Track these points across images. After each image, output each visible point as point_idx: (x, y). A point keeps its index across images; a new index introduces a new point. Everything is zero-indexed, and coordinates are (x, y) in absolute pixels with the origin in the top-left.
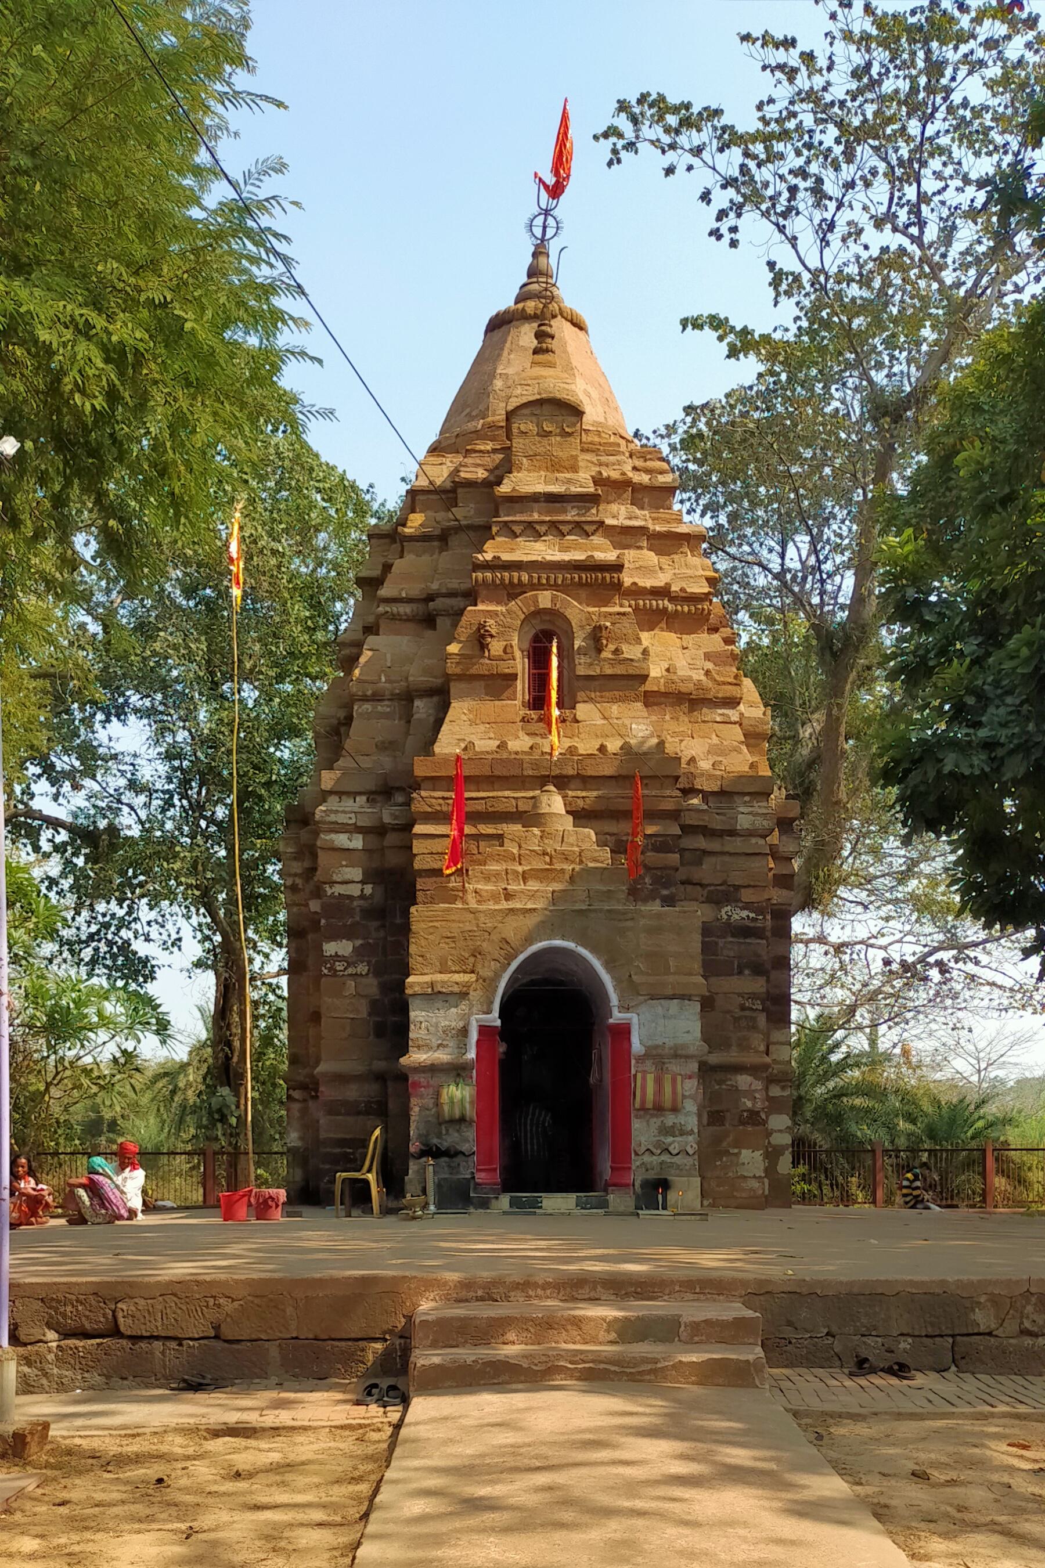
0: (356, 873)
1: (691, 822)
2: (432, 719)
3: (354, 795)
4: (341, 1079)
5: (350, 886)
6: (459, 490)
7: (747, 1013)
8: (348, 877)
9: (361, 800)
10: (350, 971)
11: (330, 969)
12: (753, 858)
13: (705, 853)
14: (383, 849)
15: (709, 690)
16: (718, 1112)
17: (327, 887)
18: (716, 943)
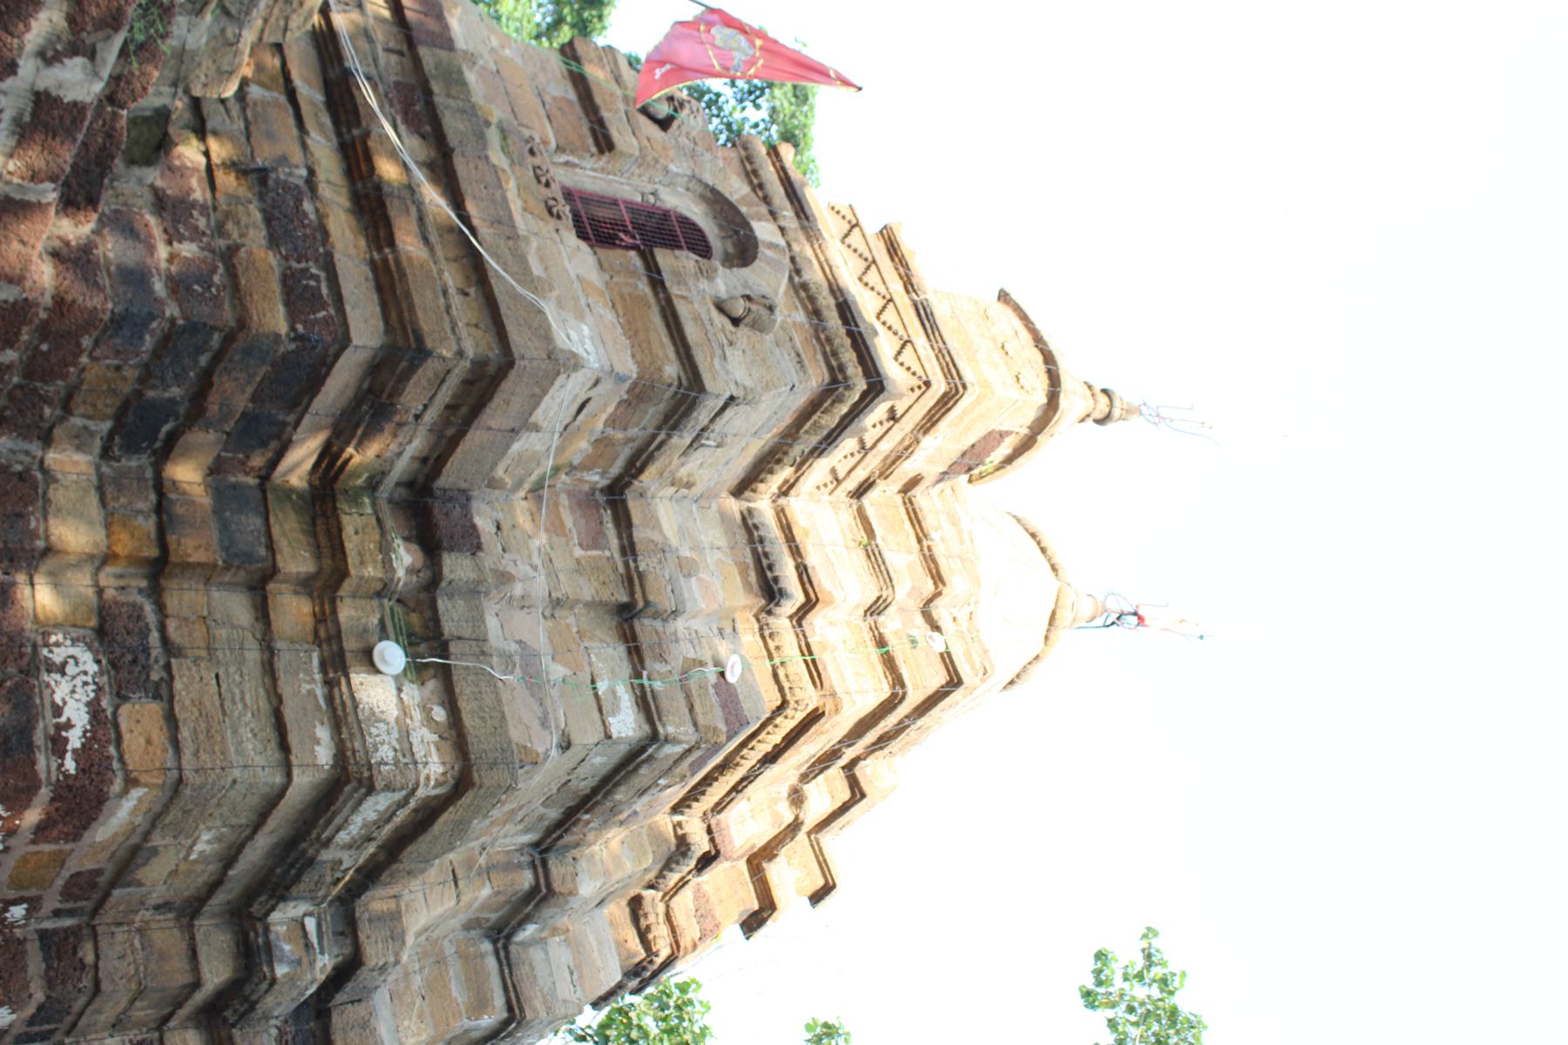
12: (270, 733)
13: (259, 588)
15: (661, 658)
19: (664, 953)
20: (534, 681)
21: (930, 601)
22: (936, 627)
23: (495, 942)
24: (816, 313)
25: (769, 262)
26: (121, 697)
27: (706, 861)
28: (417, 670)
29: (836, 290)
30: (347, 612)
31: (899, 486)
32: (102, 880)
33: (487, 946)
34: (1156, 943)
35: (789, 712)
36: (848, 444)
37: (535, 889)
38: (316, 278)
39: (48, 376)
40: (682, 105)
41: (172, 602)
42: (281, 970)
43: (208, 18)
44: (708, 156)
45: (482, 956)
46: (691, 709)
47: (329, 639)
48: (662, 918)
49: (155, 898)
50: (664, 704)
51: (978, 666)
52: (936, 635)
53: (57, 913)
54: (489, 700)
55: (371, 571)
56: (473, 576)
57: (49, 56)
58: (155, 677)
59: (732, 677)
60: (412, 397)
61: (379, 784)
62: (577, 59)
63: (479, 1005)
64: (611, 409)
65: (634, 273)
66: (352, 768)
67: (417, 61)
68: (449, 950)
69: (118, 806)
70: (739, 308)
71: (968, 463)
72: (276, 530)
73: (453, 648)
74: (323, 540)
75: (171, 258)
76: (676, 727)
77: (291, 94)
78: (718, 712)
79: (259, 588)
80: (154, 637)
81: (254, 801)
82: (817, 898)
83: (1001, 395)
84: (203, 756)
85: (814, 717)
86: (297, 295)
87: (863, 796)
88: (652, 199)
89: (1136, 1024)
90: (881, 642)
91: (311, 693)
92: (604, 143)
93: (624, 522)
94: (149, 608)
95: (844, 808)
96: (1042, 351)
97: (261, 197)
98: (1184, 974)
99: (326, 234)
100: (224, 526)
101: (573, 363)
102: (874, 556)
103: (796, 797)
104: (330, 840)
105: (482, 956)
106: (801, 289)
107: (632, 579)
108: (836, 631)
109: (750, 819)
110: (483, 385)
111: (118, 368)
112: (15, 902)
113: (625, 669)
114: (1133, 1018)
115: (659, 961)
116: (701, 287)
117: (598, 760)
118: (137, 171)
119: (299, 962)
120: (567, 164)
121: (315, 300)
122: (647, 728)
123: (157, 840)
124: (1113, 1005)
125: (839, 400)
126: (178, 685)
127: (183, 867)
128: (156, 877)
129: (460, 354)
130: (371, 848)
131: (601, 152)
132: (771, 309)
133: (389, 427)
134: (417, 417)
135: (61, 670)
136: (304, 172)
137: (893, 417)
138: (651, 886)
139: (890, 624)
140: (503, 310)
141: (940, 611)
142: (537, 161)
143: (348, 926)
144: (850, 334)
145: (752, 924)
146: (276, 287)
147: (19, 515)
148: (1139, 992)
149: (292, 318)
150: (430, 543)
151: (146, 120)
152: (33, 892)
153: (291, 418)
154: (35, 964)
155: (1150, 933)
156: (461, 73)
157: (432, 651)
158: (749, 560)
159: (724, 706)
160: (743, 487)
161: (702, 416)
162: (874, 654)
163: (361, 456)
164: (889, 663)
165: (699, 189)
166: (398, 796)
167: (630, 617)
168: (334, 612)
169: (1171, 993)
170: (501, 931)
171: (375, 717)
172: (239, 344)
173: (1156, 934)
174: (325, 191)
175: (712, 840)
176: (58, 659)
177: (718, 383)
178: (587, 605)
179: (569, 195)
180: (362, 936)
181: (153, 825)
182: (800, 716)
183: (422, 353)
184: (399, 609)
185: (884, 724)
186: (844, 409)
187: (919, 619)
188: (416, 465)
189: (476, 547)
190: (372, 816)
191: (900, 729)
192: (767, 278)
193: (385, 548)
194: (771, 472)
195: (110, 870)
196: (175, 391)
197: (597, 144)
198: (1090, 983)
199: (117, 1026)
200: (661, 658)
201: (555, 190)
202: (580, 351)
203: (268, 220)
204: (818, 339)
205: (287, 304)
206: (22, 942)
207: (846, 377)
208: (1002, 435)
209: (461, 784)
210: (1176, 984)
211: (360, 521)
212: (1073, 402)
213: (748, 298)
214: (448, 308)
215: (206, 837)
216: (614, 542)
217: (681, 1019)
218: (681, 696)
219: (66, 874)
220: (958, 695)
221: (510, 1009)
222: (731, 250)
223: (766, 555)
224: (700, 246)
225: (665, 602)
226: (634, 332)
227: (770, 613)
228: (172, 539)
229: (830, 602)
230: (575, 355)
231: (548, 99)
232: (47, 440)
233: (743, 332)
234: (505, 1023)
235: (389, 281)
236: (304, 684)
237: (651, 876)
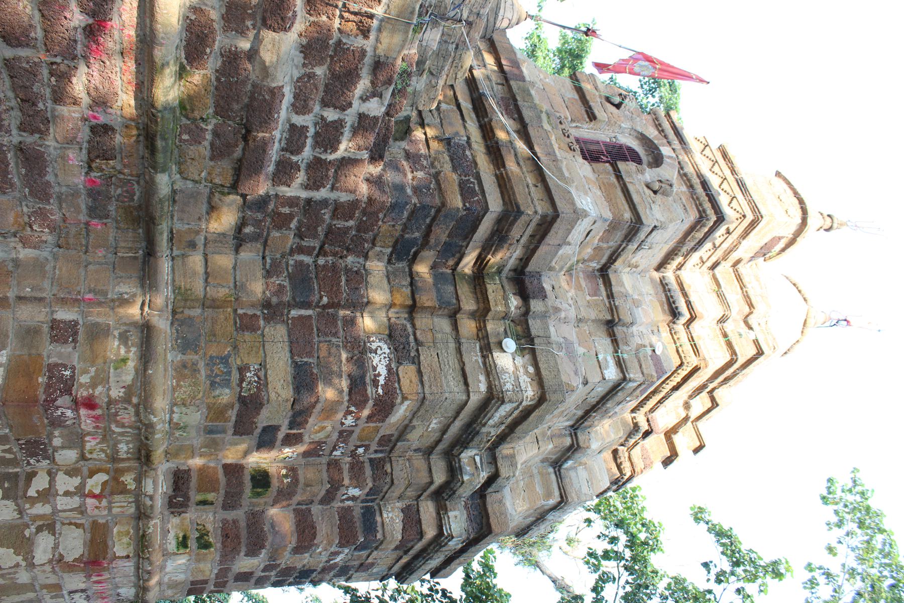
1: (490, 291)
7: (235, 376)
12: (460, 378)
13: (453, 316)
15: (627, 344)
16: (76, 333)
18: (335, 335)
19: (628, 474)
20: (571, 355)
21: (748, 316)
22: (751, 328)
23: (554, 468)
24: (691, 186)
25: (669, 164)
26: (399, 363)
27: (647, 434)
28: (521, 350)
29: (700, 176)
30: (490, 326)
31: (731, 264)
32: (393, 439)
33: (551, 470)
34: (858, 475)
35: (684, 367)
36: (708, 245)
37: (572, 446)
38: (473, 183)
39: (366, 231)
40: (625, 97)
41: (418, 323)
42: (466, 478)
43: (425, 76)
44: (638, 119)
45: (549, 474)
46: (641, 367)
47: (483, 338)
48: (627, 459)
49: (414, 447)
50: (628, 364)
51: (771, 345)
52: (751, 331)
53: (376, 452)
54: (552, 363)
55: (500, 308)
56: (543, 309)
57: (364, 99)
58: (412, 354)
59: (658, 352)
60: (515, 232)
61: (506, 400)
62: (577, 80)
63: (548, 495)
64: (601, 234)
65: (608, 173)
66: (495, 393)
67: (510, 88)
68: (535, 471)
69: (400, 408)
70: (656, 186)
71: (764, 252)
72: (459, 292)
73: (536, 341)
74: (479, 296)
75: (413, 179)
76: (634, 374)
77: (458, 106)
78: (653, 368)
79: (453, 316)
80: (412, 338)
81: (454, 407)
82: (696, 451)
83: (779, 220)
84: (433, 388)
85: (696, 369)
86: (466, 191)
87: (717, 405)
88: (614, 140)
89: (849, 513)
90: (725, 335)
91: (476, 361)
92: (592, 117)
93: (608, 284)
94: (409, 326)
95: (708, 411)
96: (798, 198)
97: (449, 150)
98: (873, 491)
99: (476, 164)
100: (438, 291)
101: (585, 214)
102: (721, 296)
103: (687, 406)
104: (486, 423)
105: (549, 474)
106: (684, 176)
107: (613, 309)
108: (705, 330)
109: (667, 415)
110: (546, 225)
111: (394, 226)
112: (360, 447)
114: (847, 510)
115: (626, 478)
116: (638, 177)
117: (599, 389)
118: (398, 143)
119: (473, 475)
120: (576, 127)
121: (473, 193)
122: (621, 375)
123: (415, 423)
124: (837, 504)
125: (704, 225)
126: (422, 358)
127: (425, 434)
128: (415, 438)
129: (536, 212)
130: (503, 427)
131: (591, 121)
132: (671, 186)
133: (506, 246)
134: (518, 241)
136: (465, 138)
137: (728, 232)
138: (622, 445)
139: (729, 327)
140: (553, 192)
141: (752, 320)
142: (563, 127)
143: (494, 460)
144: (707, 195)
145: (667, 462)
146: (457, 188)
147: (357, 289)
148: (850, 498)
149: (464, 201)
150: (524, 295)
151: (401, 121)
152: (367, 443)
153: (464, 244)
154: (368, 471)
155: (855, 471)
156: (529, 91)
157: (527, 342)
158: (664, 299)
159: (655, 365)
160: (660, 267)
161: (642, 235)
162: (722, 341)
163: (494, 259)
164: (729, 345)
165: (635, 134)
166: (515, 405)
167: (611, 326)
168: (485, 326)
169: (866, 499)
170: (557, 464)
171: (504, 371)
172: (442, 213)
173: (858, 471)
174: (475, 146)
175: (649, 425)
176: (374, 348)
177: (649, 221)
178: (593, 321)
179: (578, 140)
180: (499, 465)
181: (413, 417)
182: (689, 369)
183: (519, 213)
184: (512, 324)
185: (726, 373)
186: (706, 229)
187: (743, 325)
188: (517, 262)
189: (545, 297)
190: (504, 414)
191: (734, 375)
192: (668, 172)
193: (506, 298)
194: (673, 259)
195: (396, 434)
196: (417, 234)
197: (589, 117)
198: (825, 493)
199: (400, 498)
200: (627, 344)
201: (572, 139)
202: (587, 209)
203: (452, 160)
204: (693, 198)
205: (462, 195)
206: (363, 463)
207: (707, 215)
208: (780, 238)
209: (541, 400)
210: (869, 495)
211: (494, 287)
212: (814, 221)
213: (660, 181)
214: (529, 193)
215: (434, 421)
216: (604, 293)
217: (633, 503)
218: (636, 361)
219: (379, 436)
220: (761, 359)
221: (562, 497)
222: (651, 160)
223: (672, 297)
224: (637, 160)
225: (627, 319)
226: (609, 199)
227: (674, 323)
228: (417, 296)
229: (702, 317)
230: (585, 211)
231: (566, 99)
232: (366, 257)
233: (659, 197)
234: (560, 503)
235: (504, 183)
236: (473, 358)
237: (622, 440)
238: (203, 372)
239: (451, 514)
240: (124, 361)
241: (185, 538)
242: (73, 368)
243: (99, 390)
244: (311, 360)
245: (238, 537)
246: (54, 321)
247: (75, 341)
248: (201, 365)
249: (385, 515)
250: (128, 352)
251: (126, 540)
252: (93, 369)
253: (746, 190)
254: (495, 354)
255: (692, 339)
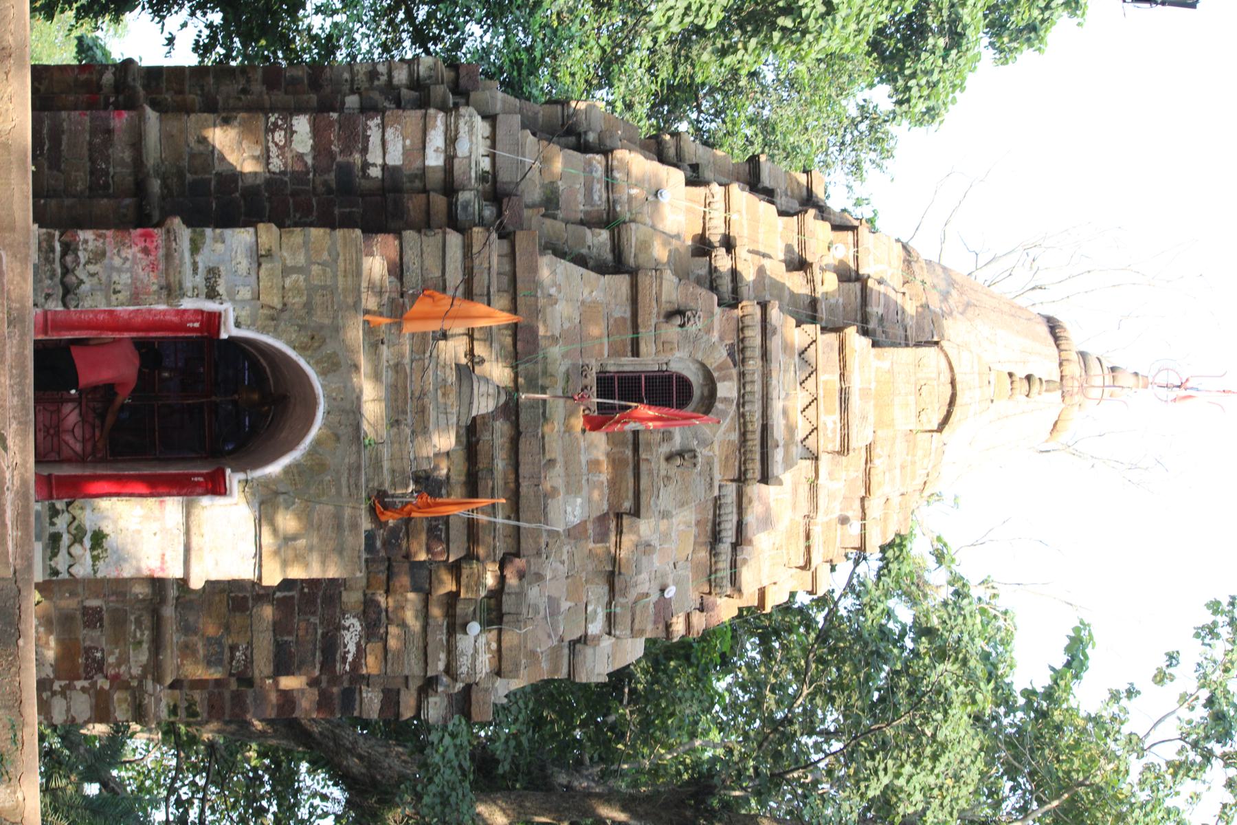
0: (395, 157)
2: (584, 251)
3: (493, 157)
4: (137, 143)
5: (379, 152)
6: (858, 285)
8: (390, 148)
9: (486, 164)
10: (273, 149)
11: (275, 124)
12: (421, 656)
14: (425, 191)
15: (624, 596)
16: (101, 619)
17: (378, 120)
18: (314, 613)
26: (368, 641)
30: (460, 608)
38: (441, 530)
46: (633, 621)
73: (505, 619)
78: (652, 618)
88: (664, 368)
90: (808, 537)
113: (606, 599)
135: (348, 629)
171: (462, 654)
200: (624, 596)
226: (614, 484)
238: (201, 652)
239: (431, 700)
240: (140, 643)
241: (175, 706)
242: (103, 650)
243: (123, 668)
244: (289, 638)
245: (222, 708)
246: (84, 608)
247: (101, 626)
248: (200, 645)
249: (364, 695)
250: (142, 635)
251: (125, 706)
252: (117, 651)
253: (847, 408)
254: (458, 636)
255: (733, 565)
